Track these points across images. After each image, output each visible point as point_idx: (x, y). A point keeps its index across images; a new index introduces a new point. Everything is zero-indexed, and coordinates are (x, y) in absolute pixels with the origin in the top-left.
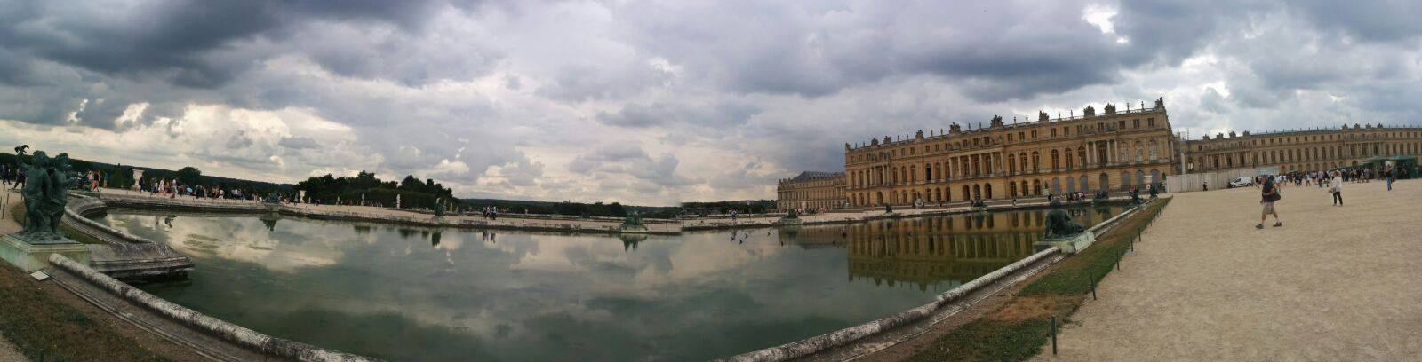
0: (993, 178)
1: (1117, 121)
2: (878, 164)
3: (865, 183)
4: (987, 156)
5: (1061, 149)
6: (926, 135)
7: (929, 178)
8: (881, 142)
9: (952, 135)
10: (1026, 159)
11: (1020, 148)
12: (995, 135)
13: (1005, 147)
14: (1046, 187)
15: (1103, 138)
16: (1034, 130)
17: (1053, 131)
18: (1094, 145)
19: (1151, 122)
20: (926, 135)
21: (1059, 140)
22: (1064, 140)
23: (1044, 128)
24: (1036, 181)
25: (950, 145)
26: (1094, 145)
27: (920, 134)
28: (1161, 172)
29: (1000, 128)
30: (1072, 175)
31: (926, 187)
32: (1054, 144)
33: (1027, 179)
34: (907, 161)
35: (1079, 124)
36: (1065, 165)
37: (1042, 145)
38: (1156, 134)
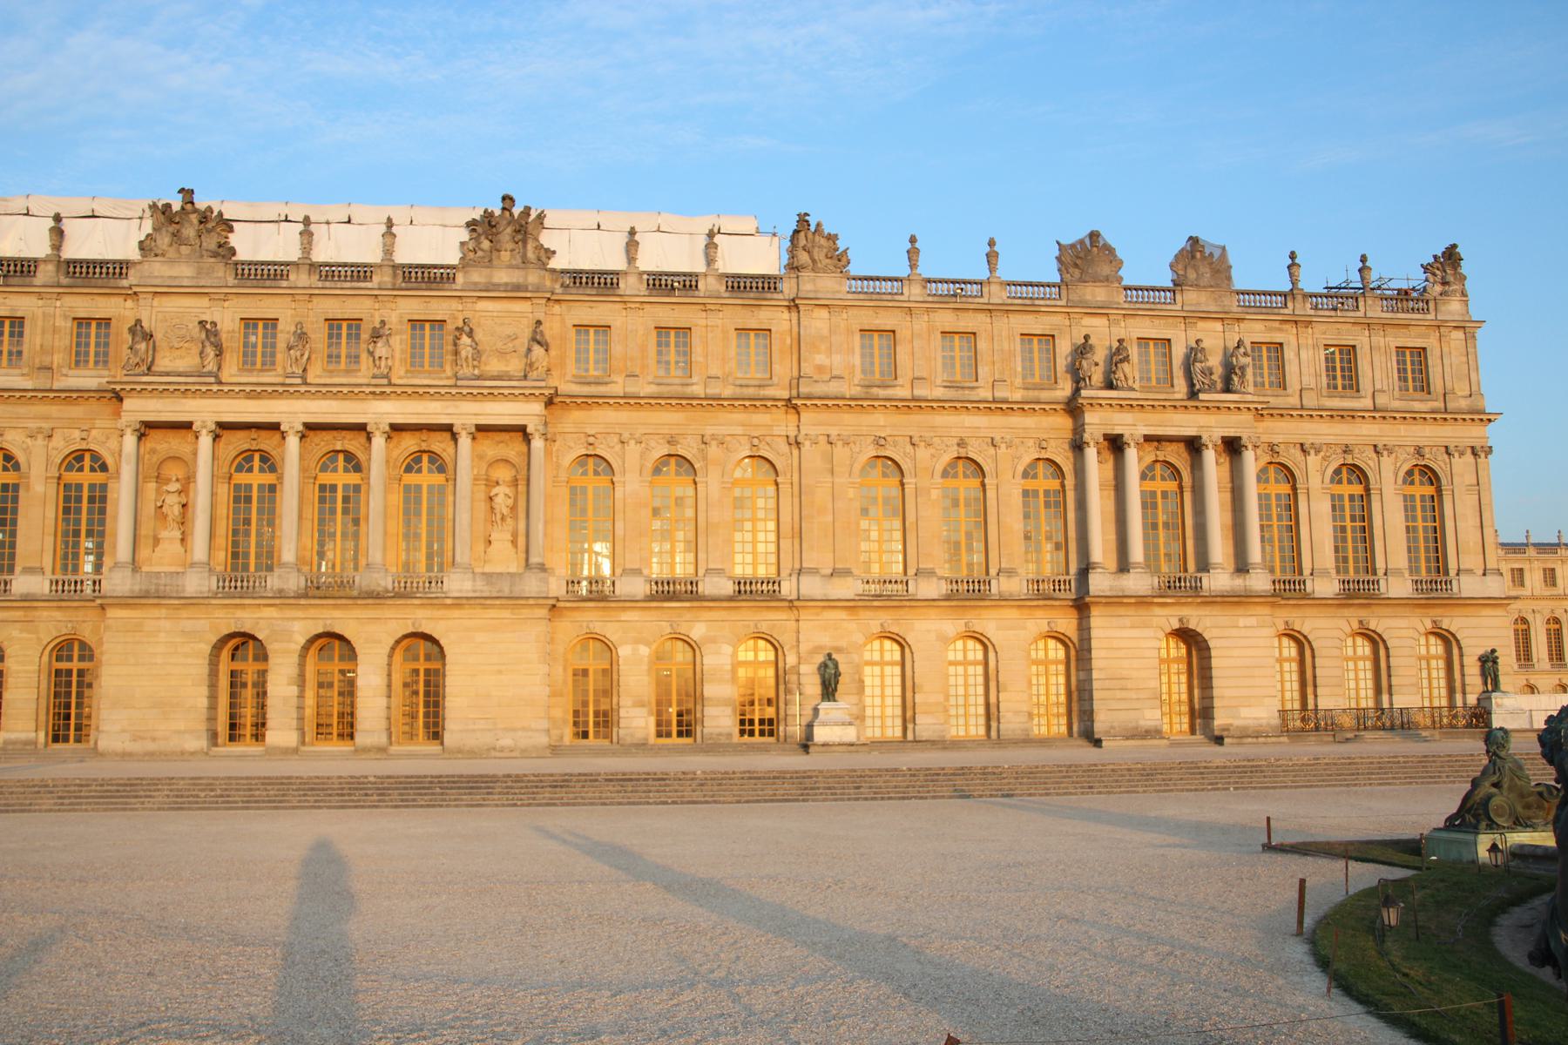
0: (459, 603)
5: (923, 453)
9: (158, 270)
11: (669, 419)
12: (499, 322)
14: (829, 689)
15: (1185, 424)
18: (1131, 454)
19: (1415, 367)
21: (914, 404)
22: (941, 405)
23: (817, 322)
25: (139, 332)
28: (1473, 650)
30: (989, 623)
32: (880, 421)
37: (812, 423)
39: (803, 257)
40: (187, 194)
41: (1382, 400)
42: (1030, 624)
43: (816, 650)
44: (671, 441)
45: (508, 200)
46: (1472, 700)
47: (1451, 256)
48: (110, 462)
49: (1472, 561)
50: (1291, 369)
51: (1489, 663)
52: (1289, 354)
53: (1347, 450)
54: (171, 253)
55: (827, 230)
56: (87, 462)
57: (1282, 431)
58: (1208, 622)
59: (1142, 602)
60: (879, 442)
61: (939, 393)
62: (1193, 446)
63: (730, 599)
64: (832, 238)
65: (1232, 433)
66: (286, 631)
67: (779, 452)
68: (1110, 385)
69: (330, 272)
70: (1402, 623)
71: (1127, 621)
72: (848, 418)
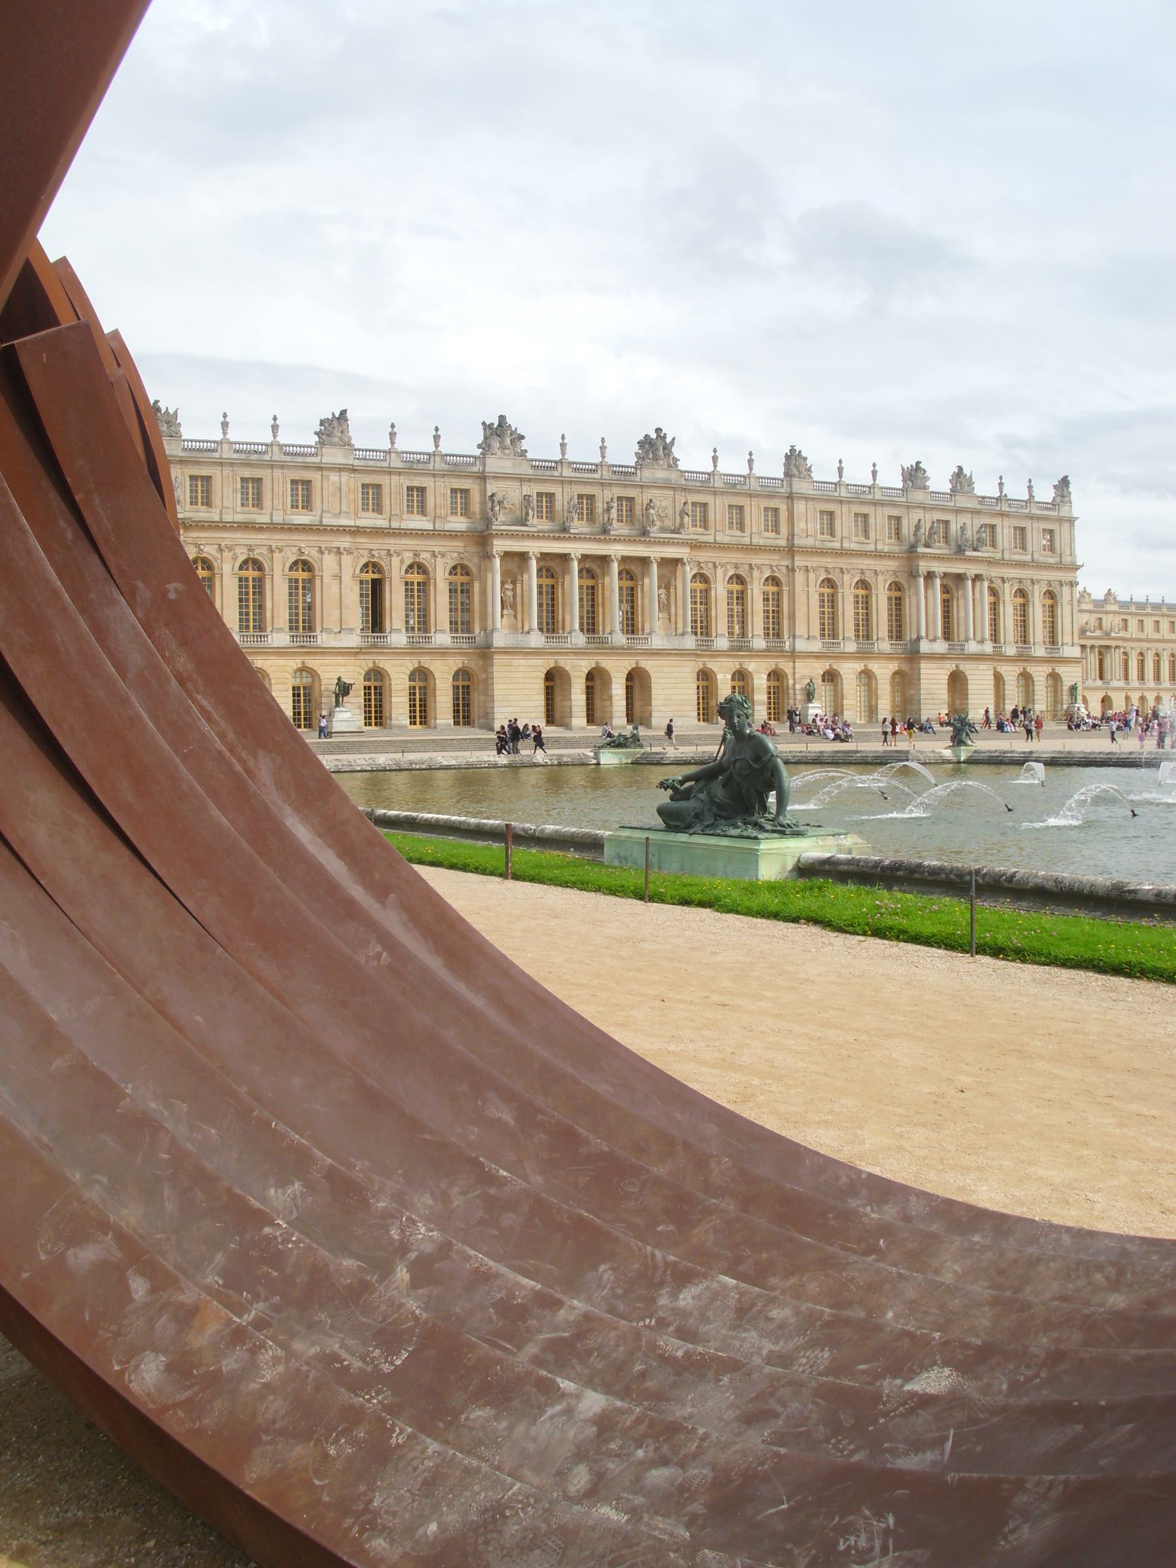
4: (633, 569)
6: (366, 435)
7: (376, 620)
12: (664, 501)
13: (696, 546)
15: (957, 568)
16: (773, 504)
18: (938, 582)
20: (366, 435)
21: (843, 553)
24: (776, 675)
26: (938, 582)
29: (673, 476)
31: (366, 663)
32: (830, 562)
34: (276, 540)
35: (895, 512)
36: (850, 633)
37: (799, 561)
39: (795, 471)
40: (502, 418)
41: (1036, 556)
42: (891, 666)
43: (803, 678)
44: (736, 567)
45: (658, 430)
46: (1065, 707)
47: (1065, 482)
48: (474, 570)
49: (1067, 639)
50: (999, 538)
51: (1073, 689)
52: (999, 530)
53: (1020, 581)
54: (499, 452)
55: (804, 454)
56: (459, 570)
57: (995, 572)
58: (967, 666)
59: (942, 657)
60: (827, 570)
61: (853, 546)
63: (764, 651)
64: (805, 459)
65: (978, 572)
66: (578, 669)
67: (781, 575)
68: (927, 546)
69: (576, 467)
70: (1040, 669)
71: (935, 666)
72: (815, 559)
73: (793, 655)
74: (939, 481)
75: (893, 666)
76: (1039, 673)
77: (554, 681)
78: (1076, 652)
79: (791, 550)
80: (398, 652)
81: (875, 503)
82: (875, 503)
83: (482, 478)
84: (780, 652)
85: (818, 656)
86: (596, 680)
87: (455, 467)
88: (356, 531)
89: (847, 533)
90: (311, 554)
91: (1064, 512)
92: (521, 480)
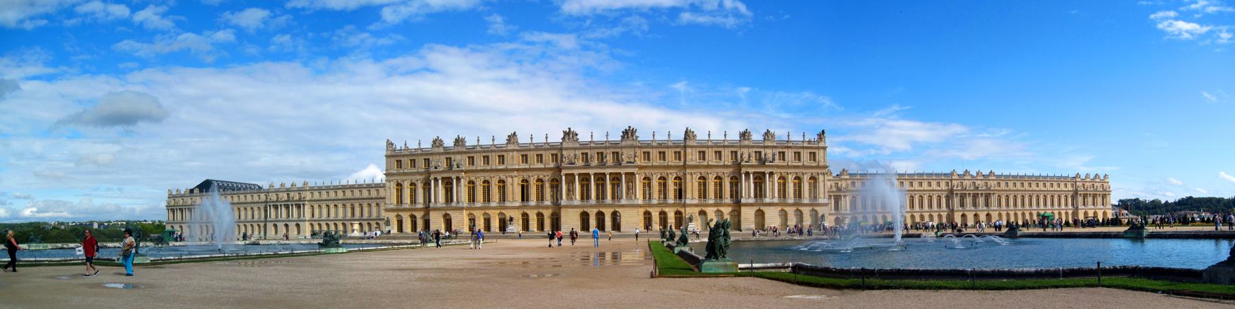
0: (623, 206)
1: (777, 151)
2: (445, 175)
3: (420, 199)
8: (449, 142)
10: (665, 185)
13: (641, 167)
17: (703, 155)
19: (813, 156)
20: (523, 139)
21: (708, 166)
24: (678, 213)
27: (512, 138)
30: (722, 209)
32: (703, 171)
33: (666, 210)
38: (820, 171)
59: (752, 205)
62: (764, 174)
73: (685, 205)
74: (757, 136)
75: (730, 209)
76: (806, 211)
77: (585, 217)
78: (826, 201)
79: (685, 167)
80: (532, 208)
81: (724, 147)
82: (724, 147)
83: (561, 149)
84: (679, 205)
85: (696, 205)
86: (600, 216)
87: (552, 147)
88: (518, 170)
89: (711, 157)
90: (503, 177)
91: (821, 145)
92: (575, 149)
